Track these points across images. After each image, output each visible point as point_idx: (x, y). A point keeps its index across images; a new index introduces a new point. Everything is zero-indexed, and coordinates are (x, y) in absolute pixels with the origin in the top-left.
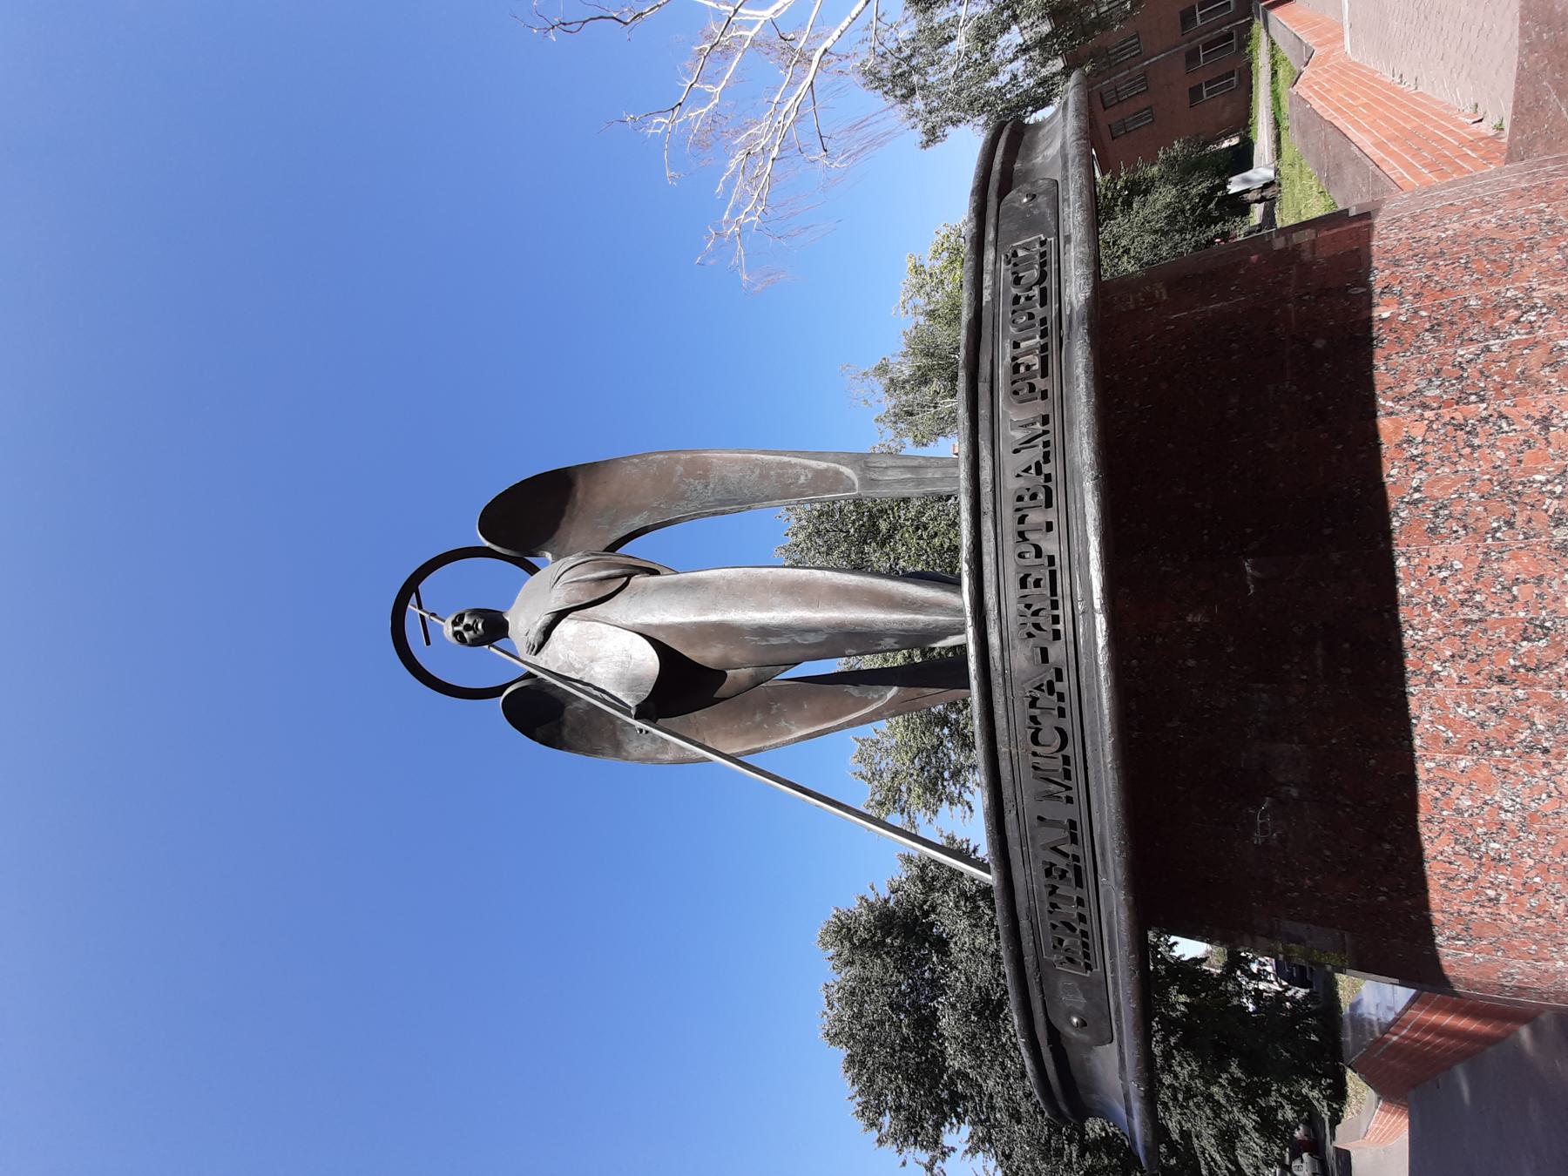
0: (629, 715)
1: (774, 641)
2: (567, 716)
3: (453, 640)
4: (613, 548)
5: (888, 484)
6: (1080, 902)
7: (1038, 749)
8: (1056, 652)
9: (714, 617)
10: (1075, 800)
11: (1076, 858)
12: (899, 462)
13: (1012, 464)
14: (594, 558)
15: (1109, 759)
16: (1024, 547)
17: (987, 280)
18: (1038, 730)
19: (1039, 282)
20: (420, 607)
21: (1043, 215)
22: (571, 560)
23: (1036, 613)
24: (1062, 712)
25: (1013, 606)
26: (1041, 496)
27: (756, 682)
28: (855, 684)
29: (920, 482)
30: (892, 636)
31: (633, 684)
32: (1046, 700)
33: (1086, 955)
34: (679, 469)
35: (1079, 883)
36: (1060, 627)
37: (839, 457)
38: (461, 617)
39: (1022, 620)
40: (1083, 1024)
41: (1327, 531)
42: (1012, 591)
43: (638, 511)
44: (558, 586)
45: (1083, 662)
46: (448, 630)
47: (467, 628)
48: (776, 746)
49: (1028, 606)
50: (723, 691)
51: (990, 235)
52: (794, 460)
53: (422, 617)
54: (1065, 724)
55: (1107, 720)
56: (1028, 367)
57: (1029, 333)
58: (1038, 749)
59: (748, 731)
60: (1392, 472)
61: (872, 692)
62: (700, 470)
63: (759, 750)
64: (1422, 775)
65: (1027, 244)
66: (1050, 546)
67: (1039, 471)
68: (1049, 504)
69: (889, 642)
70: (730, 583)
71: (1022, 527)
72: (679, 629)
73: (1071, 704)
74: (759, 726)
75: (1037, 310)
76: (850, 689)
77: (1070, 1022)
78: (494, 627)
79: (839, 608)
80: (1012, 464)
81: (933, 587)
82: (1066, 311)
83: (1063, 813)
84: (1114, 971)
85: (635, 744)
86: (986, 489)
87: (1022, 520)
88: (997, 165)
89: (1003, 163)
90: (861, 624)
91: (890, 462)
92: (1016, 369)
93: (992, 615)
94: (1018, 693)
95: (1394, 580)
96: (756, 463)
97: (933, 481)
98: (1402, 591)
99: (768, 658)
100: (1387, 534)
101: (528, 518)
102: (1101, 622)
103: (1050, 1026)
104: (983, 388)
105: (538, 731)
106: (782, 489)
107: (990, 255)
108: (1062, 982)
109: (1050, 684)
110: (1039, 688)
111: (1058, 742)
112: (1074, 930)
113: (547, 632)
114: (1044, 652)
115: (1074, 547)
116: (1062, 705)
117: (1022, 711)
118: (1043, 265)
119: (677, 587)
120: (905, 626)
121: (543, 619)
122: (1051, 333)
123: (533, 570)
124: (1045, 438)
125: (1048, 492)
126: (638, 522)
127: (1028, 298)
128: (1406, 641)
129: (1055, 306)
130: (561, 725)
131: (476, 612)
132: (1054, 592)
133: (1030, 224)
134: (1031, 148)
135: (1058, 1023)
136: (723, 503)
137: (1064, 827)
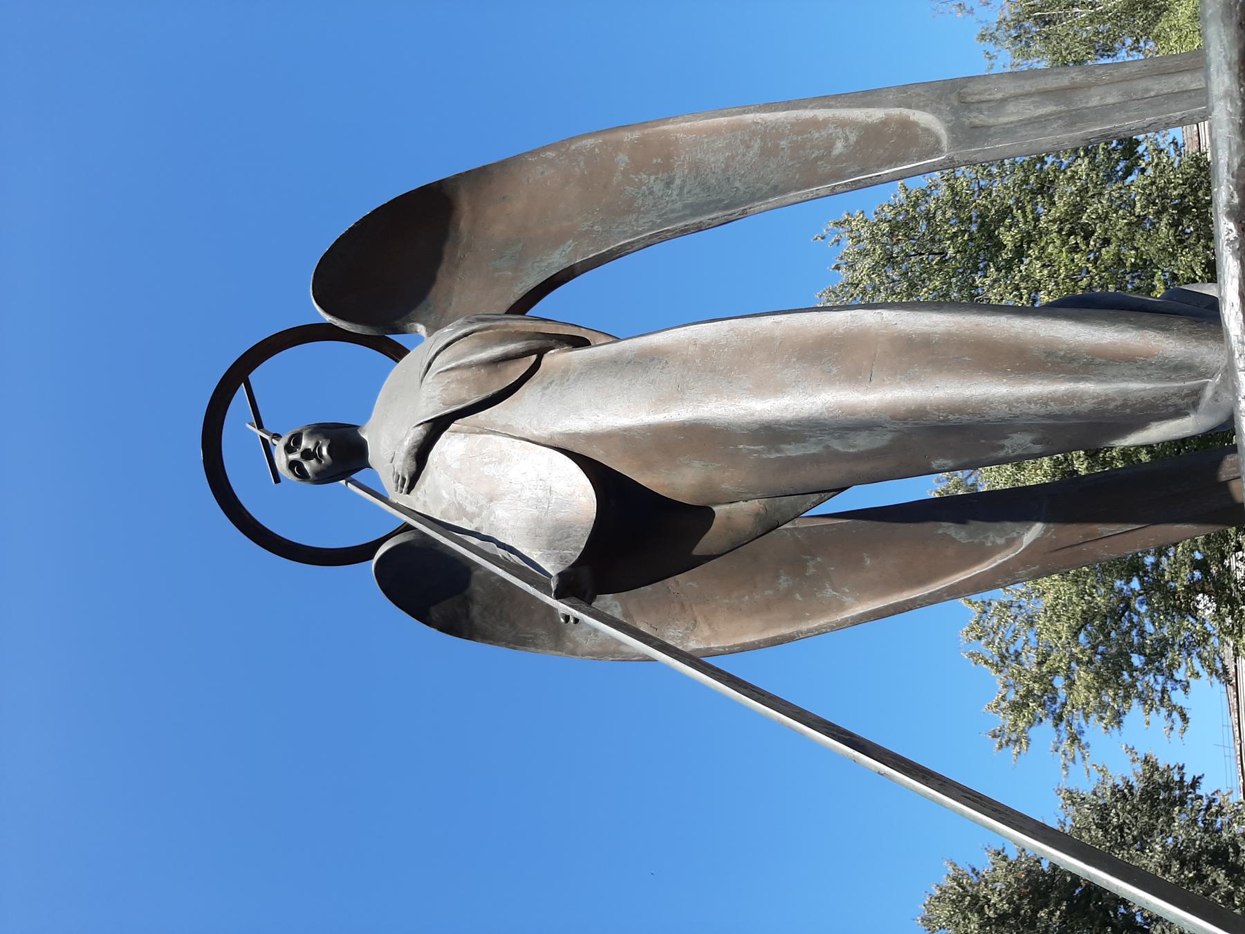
0: (547, 590)
1: (792, 451)
2: (476, 587)
4: (521, 307)
5: (1008, 131)
12: (1028, 86)
20: (260, 427)
22: (447, 333)
27: (768, 525)
29: (1073, 118)
30: (1027, 429)
31: (556, 535)
34: (623, 159)
37: (907, 95)
38: (296, 438)
43: (557, 240)
44: (429, 378)
47: (307, 455)
48: (819, 632)
52: (821, 114)
59: (767, 606)
61: (993, 534)
62: (657, 158)
63: (790, 639)
69: (1019, 441)
70: (706, 350)
74: (787, 596)
76: (950, 529)
78: (346, 453)
79: (911, 379)
81: (1113, 321)
91: (1010, 88)
96: (753, 131)
97: (1104, 112)
101: (385, 272)
105: (435, 612)
106: (806, 168)
113: (421, 454)
119: (617, 365)
120: (1054, 408)
121: (412, 435)
123: (397, 353)
126: (557, 261)
130: (467, 601)
131: (320, 430)
136: (696, 210)
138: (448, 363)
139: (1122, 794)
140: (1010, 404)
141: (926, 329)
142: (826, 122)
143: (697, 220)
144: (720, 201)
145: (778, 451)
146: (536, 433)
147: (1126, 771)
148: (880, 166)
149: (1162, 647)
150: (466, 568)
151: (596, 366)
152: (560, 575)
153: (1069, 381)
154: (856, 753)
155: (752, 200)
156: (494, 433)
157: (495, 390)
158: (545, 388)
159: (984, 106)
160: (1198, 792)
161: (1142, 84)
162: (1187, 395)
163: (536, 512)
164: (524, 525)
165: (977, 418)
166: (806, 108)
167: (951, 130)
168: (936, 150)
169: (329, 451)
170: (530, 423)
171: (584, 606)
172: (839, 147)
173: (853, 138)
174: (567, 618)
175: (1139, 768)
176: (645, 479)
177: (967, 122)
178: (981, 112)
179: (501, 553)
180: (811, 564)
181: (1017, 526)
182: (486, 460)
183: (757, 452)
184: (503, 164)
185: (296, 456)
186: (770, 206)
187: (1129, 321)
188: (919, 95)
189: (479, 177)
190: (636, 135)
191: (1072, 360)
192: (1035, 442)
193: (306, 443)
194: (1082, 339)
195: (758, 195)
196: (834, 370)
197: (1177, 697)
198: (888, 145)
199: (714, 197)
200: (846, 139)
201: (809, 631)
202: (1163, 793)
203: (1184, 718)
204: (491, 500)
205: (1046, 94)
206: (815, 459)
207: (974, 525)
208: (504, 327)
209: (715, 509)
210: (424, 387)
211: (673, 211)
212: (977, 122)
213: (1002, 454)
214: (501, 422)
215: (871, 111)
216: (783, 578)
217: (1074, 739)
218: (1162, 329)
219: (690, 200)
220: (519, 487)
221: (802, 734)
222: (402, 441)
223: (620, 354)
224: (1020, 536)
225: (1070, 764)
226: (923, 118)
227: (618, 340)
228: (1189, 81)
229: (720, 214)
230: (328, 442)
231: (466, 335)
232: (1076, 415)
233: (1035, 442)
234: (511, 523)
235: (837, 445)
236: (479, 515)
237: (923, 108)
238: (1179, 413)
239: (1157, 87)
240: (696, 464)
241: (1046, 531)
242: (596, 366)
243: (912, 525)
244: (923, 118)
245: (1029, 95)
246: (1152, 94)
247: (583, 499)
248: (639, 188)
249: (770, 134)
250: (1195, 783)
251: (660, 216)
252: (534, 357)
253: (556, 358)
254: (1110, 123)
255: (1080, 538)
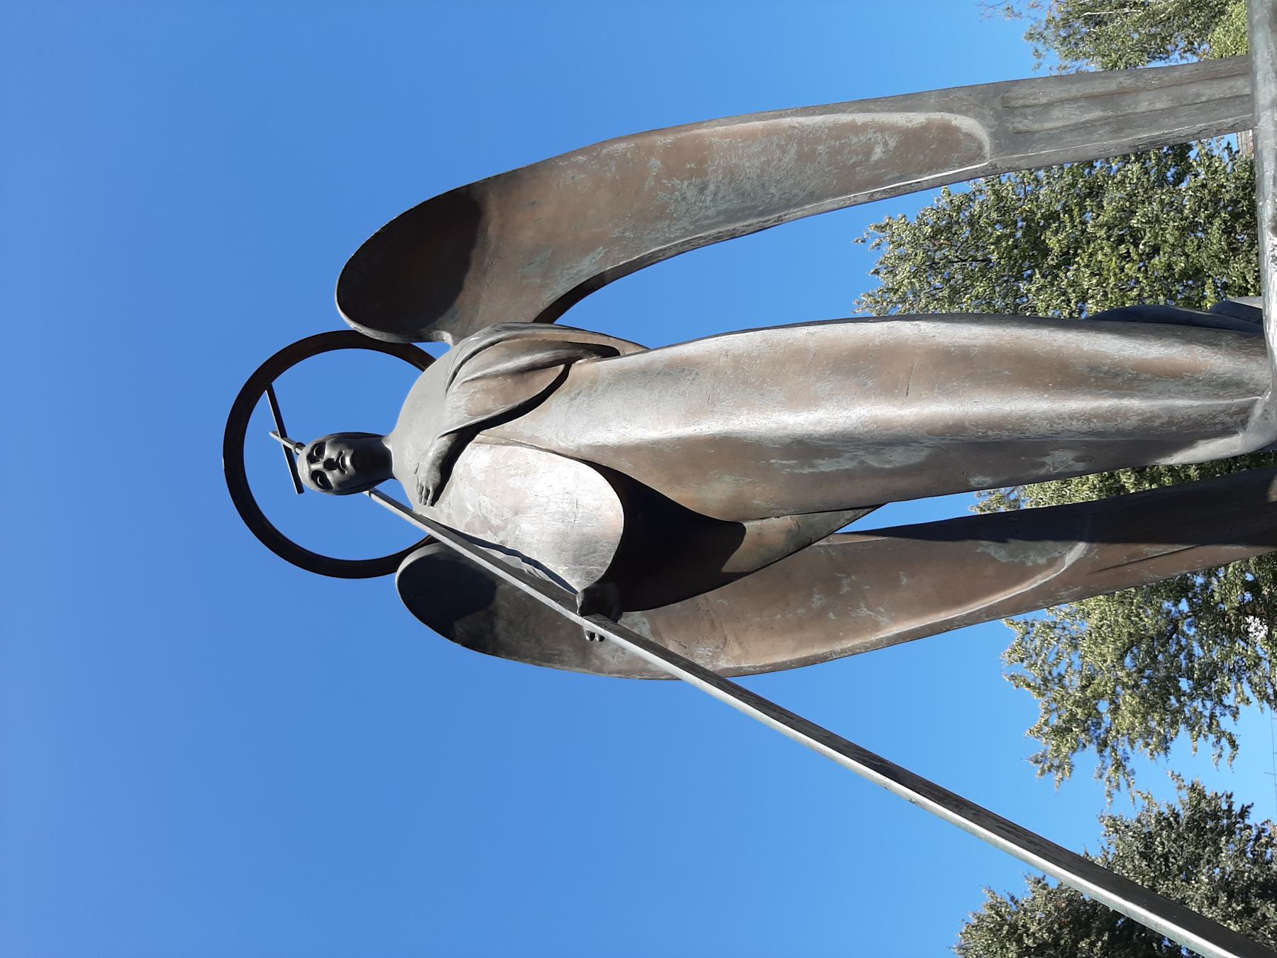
0: (572, 607)
1: (825, 466)
2: (500, 601)
4: (550, 315)
5: (1053, 137)
12: (1075, 90)
20: (283, 435)
22: (474, 342)
27: (801, 543)
29: (1121, 124)
31: (582, 550)
34: (655, 163)
37: (949, 99)
38: (319, 448)
43: (590, 246)
47: (330, 465)
48: (853, 652)
50: (736, 561)
52: (860, 118)
53: (288, 450)
59: (800, 625)
61: (1034, 553)
62: (688, 163)
63: (823, 659)
72: (654, 451)
74: (821, 614)
78: (369, 463)
79: (949, 394)
81: (1159, 335)
90: (998, 424)
91: (1056, 92)
96: (791, 135)
97: (1152, 118)
101: (411, 277)
105: (459, 627)
106: (841, 174)
113: (446, 465)
119: (646, 376)
120: (1097, 425)
121: (436, 446)
123: (423, 361)
126: (586, 268)
130: (492, 615)
131: (343, 439)
136: (730, 216)
138: (474, 372)
139: (1167, 822)
140: (1051, 421)
141: (965, 342)
142: (864, 127)
143: (731, 227)
144: (754, 208)
145: (812, 466)
146: (563, 445)
147: (1172, 799)
148: (920, 173)
149: (1211, 671)
150: (491, 582)
151: (625, 377)
152: (585, 591)
153: (1112, 396)
154: (888, 780)
155: (788, 207)
156: (520, 444)
157: (521, 401)
158: (572, 399)
159: (1029, 111)
160: (1247, 821)
161: (1193, 89)
162: (1236, 413)
163: (561, 526)
164: (550, 539)
165: (1017, 435)
166: (844, 111)
167: (994, 135)
168: (979, 156)
169: (352, 461)
170: (557, 435)
171: (610, 623)
172: (878, 152)
173: (892, 143)
174: (592, 636)
176: (673, 494)
177: (1011, 128)
178: (1025, 117)
179: (526, 567)
180: (845, 582)
181: (1059, 546)
182: (512, 472)
183: (789, 466)
184: (533, 168)
185: (318, 466)
186: (806, 213)
187: (1174, 335)
188: (961, 99)
189: (508, 181)
190: (670, 139)
191: (1116, 375)
192: (1077, 460)
193: (329, 453)
194: (1127, 353)
195: (794, 202)
196: (870, 384)
197: (1226, 723)
199: (749, 204)
200: (886, 144)
201: (843, 651)
202: (1210, 822)
203: (1233, 744)
204: (516, 513)
205: (1093, 99)
206: (848, 475)
207: (1014, 544)
208: (533, 335)
209: (745, 524)
210: (449, 397)
211: (706, 218)
212: (1021, 127)
213: (1042, 471)
214: (527, 433)
215: (911, 115)
216: (817, 596)
217: (1119, 766)
218: (1210, 344)
219: (725, 206)
220: (544, 500)
221: (833, 759)
222: (427, 451)
223: (650, 364)
224: (1062, 556)
225: (1114, 791)
226: (965, 123)
227: (648, 350)
228: (1240, 86)
229: (755, 220)
230: (351, 452)
231: (492, 344)
232: (1120, 432)
233: (1077, 460)
234: (536, 537)
235: (872, 461)
236: (504, 528)
237: (965, 112)
238: (1227, 431)
239: (1208, 91)
240: (727, 478)
241: (1090, 551)
242: (625, 377)
243: (950, 543)
244: (965, 123)
245: (1075, 100)
246: (1204, 99)
247: (610, 514)
248: (672, 193)
249: (807, 139)
250: (1244, 812)
251: (692, 223)
252: (562, 367)
253: (583, 368)
254: (1159, 129)
255: (1124, 559)
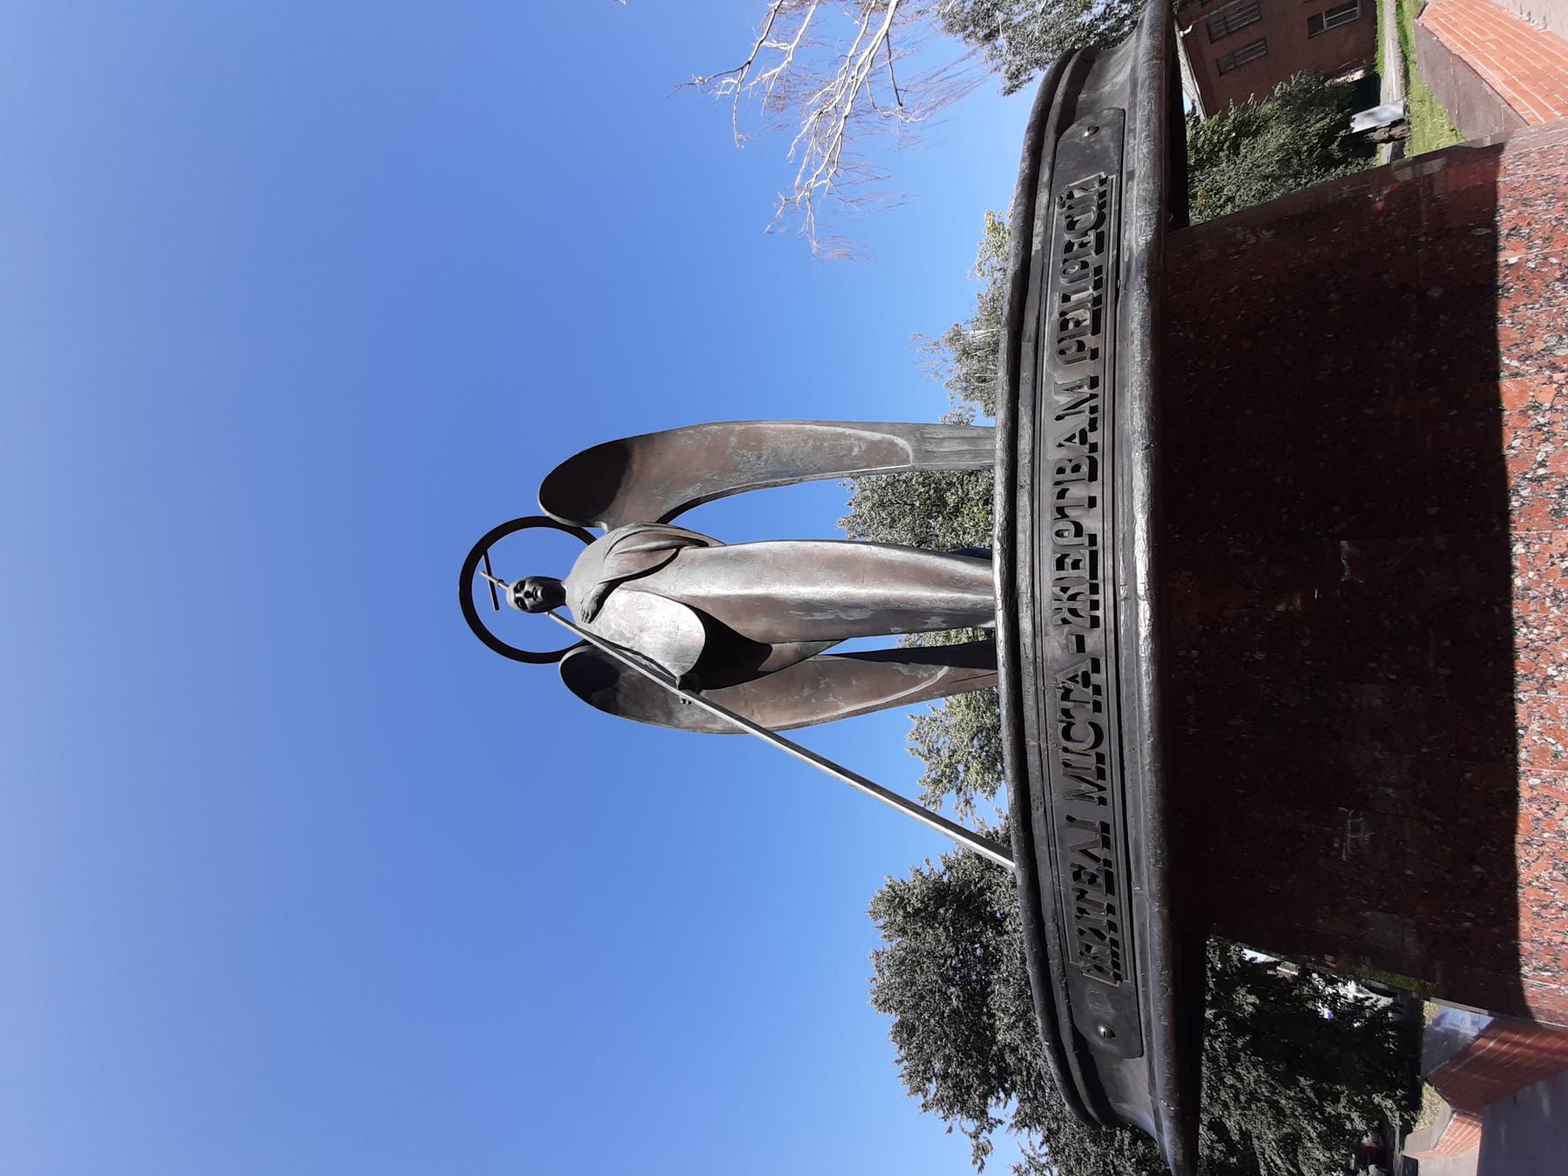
0: (672, 683)
1: (818, 616)
2: (621, 682)
3: (515, 607)
4: (665, 519)
5: (944, 456)
6: (1111, 909)
7: (1070, 745)
8: (1094, 640)
9: (758, 591)
10: (1109, 801)
11: (1107, 863)
12: (956, 433)
13: (1054, 431)
14: (645, 530)
15: (1147, 760)
16: (1062, 525)
17: (1038, 227)
18: (1070, 725)
19: (1096, 226)
21: (1106, 150)
22: (623, 531)
23: (1073, 598)
24: (1097, 707)
25: (1048, 589)
26: (1085, 469)
27: (802, 657)
28: (905, 662)
30: (939, 615)
32: (1080, 692)
33: (1116, 965)
34: (733, 440)
35: (1110, 889)
36: (1099, 613)
37: (894, 428)
38: (522, 584)
39: (1056, 604)
40: (1111, 1034)
41: (1433, 511)
42: (1048, 572)
44: (611, 556)
45: (1123, 652)
46: (510, 596)
47: (528, 595)
48: (824, 721)
49: (1064, 590)
50: (766, 665)
51: (1045, 175)
52: (848, 431)
54: (1101, 719)
55: (1146, 717)
56: (1078, 323)
57: (1081, 284)
58: (1070, 745)
59: (796, 705)
60: (1514, 444)
61: (922, 671)
62: (755, 442)
63: (807, 724)
64: (1524, 793)
65: (1085, 184)
66: (1092, 523)
67: (1083, 440)
68: (1093, 476)
69: (936, 621)
70: (776, 556)
71: (1061, 503)
72: (725, 601)
73: (1108, 698)
74: (807, 700)
75: (1093, 258)
76: (900, 667)
77: (1098, 1032)
78: (552, 595)
79: (884, 584)
80: (1054, 431)
82: (1125, 257)
83: (1097, 814)
84: (1145, 984)
85: (686, 712)
86: (1024, 461)
87: (1061, 495)
88: (1058, 97)
89: (1066, 95)
90: (906, 601)
91: (947, 433)
92: (1064, 325)
93: (1025, 598)
94: (1050, 683)
95: (1509, 570)
98: (1518, 582)
99: (813, 634)
100: (1504, 515)
101: (586, 489)
102: (1144, 610)
103: (1075, 1032)
104: (1027, 348)
106: (837, 460)
107: (1043, 198)
108: (1089, 990)
109: (1086, 676)
110: (1073, 679)
111: (1092, 739)
112: (1103, 937)
113: (600, 600)
114: (1080, 641)
115: (1120, 527)
116: (1098, 698)
117: (1053, 703)
118: (1101, 206)
119: (723, 560)
120: (952, 605)
121: (596, 589)
122: (1108, 286)
123: (589, 539)
124: (1092, 403)
125: (1093, 465)
126: (691, 493)
127: (1082, 245)
128: (1519, 640)
129: (1113, 253)
130: (616, 690)
131: (536, 580)
132: (1094, 575)
133: (1091, 160)
134: (1100, 76)
135: (1084, 1030)
136: (774, 475)
137: (1095, 830)
144: (787, 472)
175: (1003, 821)
179: (645, 662)
185: (520, 595)
189: (647, 440)
198: (880, 452)
206: (830, 622)
217: (967, 802)
226: (901, 442)
244: (901, 442)
253: (687, 552)
